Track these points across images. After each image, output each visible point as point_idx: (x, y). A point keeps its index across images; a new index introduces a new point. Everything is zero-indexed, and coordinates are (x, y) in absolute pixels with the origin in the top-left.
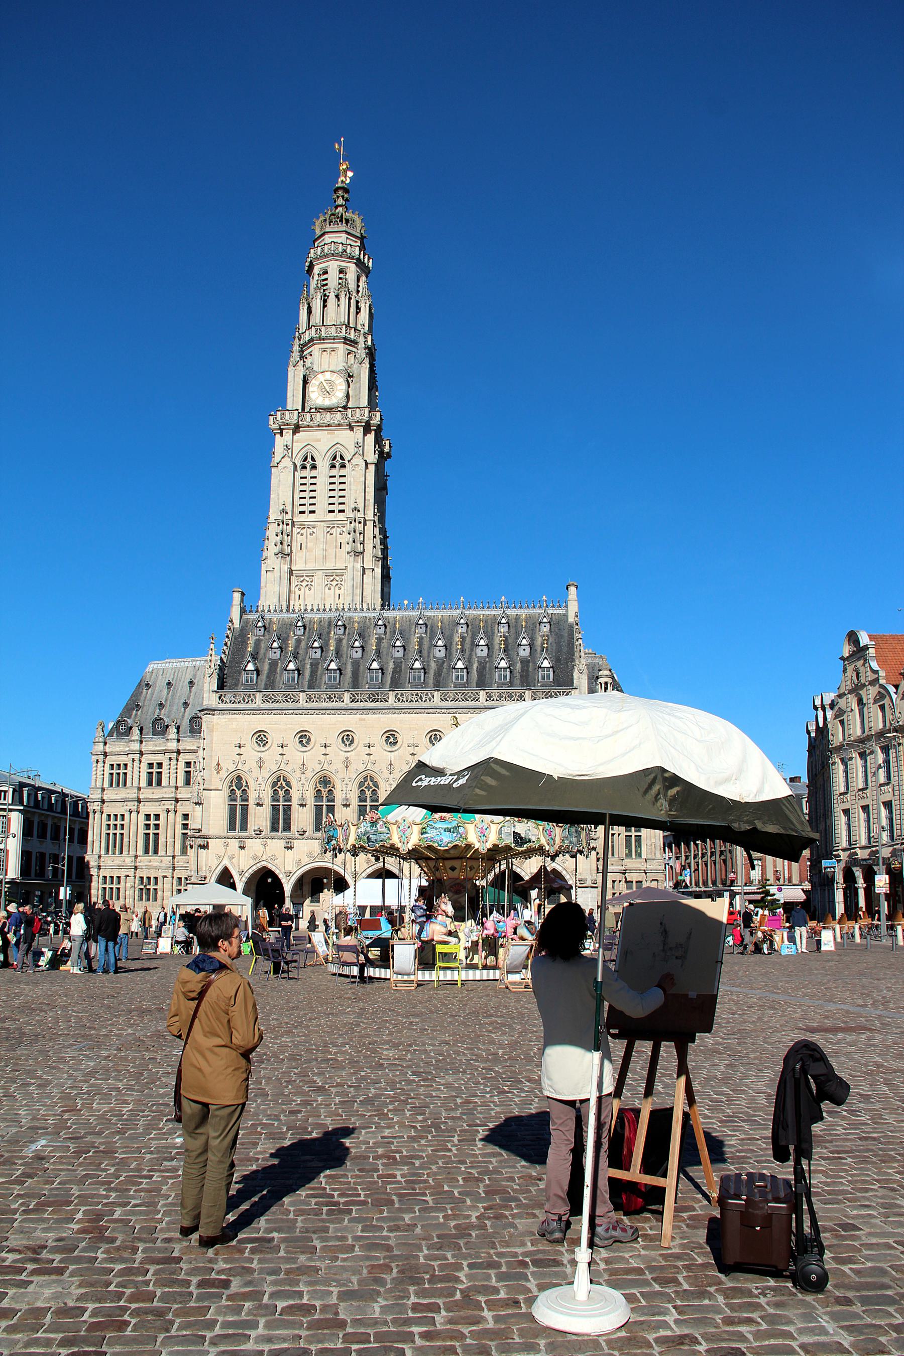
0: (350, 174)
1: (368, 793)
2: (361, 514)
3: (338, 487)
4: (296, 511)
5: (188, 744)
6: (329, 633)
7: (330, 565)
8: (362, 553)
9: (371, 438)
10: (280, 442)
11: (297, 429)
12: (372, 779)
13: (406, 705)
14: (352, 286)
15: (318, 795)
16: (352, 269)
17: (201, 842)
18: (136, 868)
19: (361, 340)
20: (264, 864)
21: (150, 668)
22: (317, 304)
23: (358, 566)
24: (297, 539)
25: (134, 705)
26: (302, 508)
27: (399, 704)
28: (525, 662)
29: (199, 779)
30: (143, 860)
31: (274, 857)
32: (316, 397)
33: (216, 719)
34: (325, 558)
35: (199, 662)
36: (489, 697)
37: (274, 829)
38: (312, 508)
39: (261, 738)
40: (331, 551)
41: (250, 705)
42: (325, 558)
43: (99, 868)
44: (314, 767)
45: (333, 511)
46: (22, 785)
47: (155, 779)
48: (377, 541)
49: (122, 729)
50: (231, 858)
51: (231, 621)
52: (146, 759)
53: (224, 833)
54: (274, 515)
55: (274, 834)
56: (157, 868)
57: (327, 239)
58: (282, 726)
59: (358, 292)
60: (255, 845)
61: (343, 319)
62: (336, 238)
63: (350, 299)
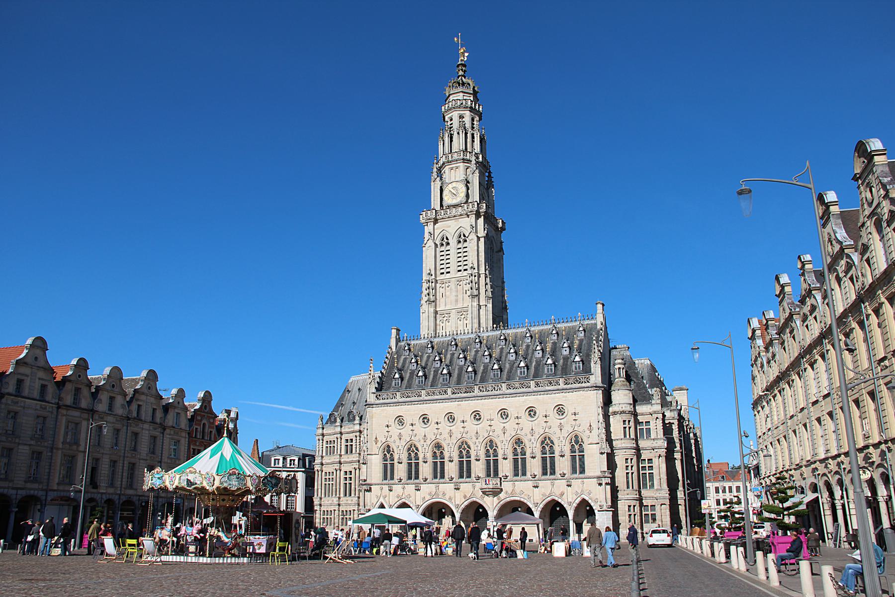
0: (466, 54)
1: (464, 453)
2: (476, 271)
3: (462, 254)
4: (438, 273)
5: (364, 425)
6: (447, 350)
7: (460, 305)
8: (478, 295)
9: (481, 221)
10: (429, 228)
11: (436, 221)
12: (466, 443)
13: (485, 393)
14: (468, 125)
15: (434, 456)
16: (467, 114)
17: (365, 487)
18: (339, 505)
19: (473, 158)
20: (403, 500)
21: (350, 381)
22: (447, 139)
23: (475, 304)
24: (440, 291)
25: (340, 404)
26: (442, 271)
27: (481, 394)
28: (566, 359)
29: (365, 448)
30: (344, 500)
31: (409, 496)
32: (448, 200)
33: (375, 410)
34: (457, 301)
35: (365, 376)
36: (537, 384)
37: (410, 478)
38: (448, 270)
39: (400, 420)
40: (460, 296)
41: (394, 400)
42: (457, 301)
43: (320, 505)
44: (431, 437)
45: (460, 271)
46: (305, 456)
47: (349, 450)
48: (489, 286)
49: (331, 420)
50: (385, 497)
51: (390, 348)
52: (344, 437)
53: (380, 482)
54: (425, 277)
55: (409, 481)
56: (350, 505)
57: (451, 98)
58: (411, 412)
59: (473, 128)
60: (398, 488)
61: (463, 147)
62: (458, 96)
63: (466, 134)
